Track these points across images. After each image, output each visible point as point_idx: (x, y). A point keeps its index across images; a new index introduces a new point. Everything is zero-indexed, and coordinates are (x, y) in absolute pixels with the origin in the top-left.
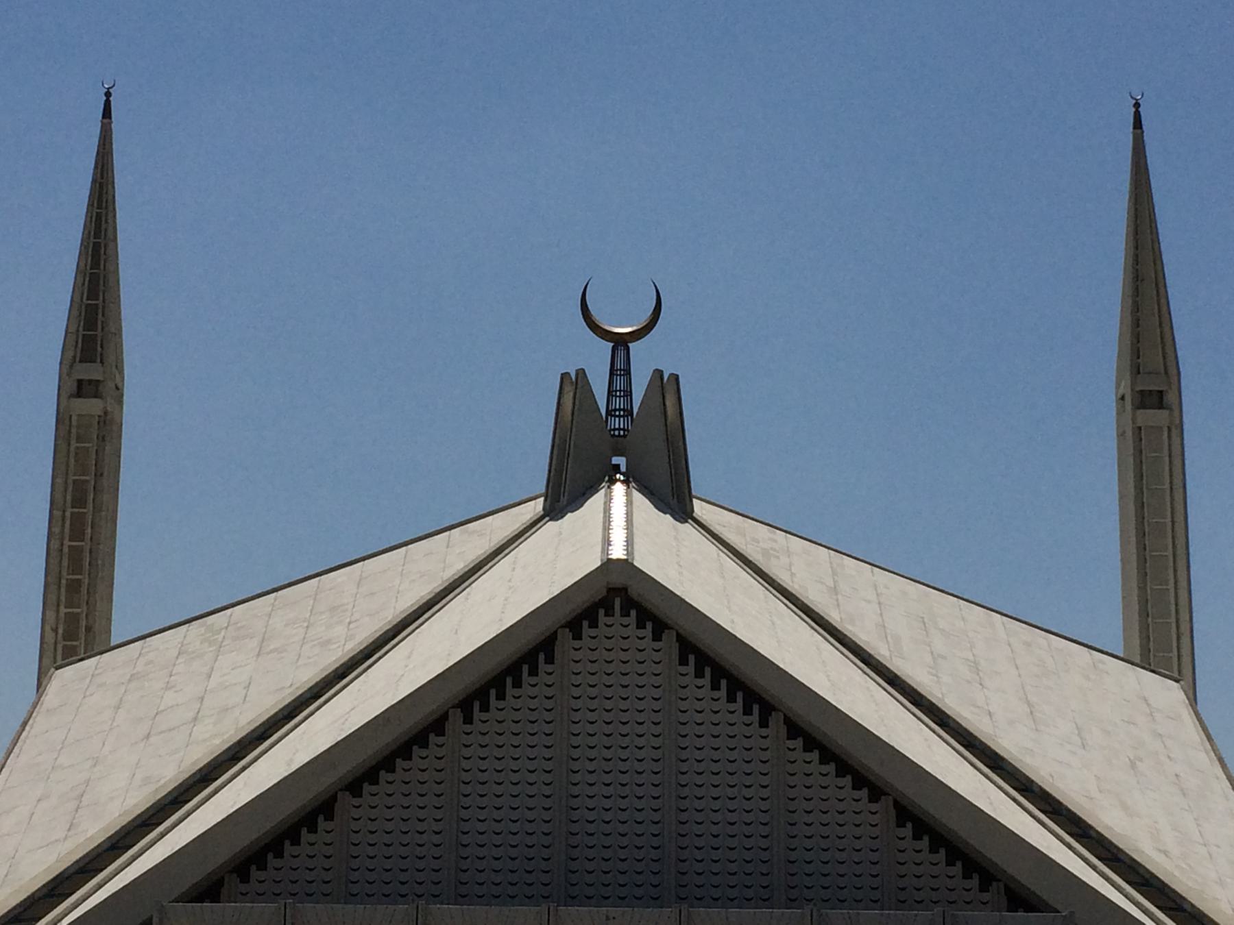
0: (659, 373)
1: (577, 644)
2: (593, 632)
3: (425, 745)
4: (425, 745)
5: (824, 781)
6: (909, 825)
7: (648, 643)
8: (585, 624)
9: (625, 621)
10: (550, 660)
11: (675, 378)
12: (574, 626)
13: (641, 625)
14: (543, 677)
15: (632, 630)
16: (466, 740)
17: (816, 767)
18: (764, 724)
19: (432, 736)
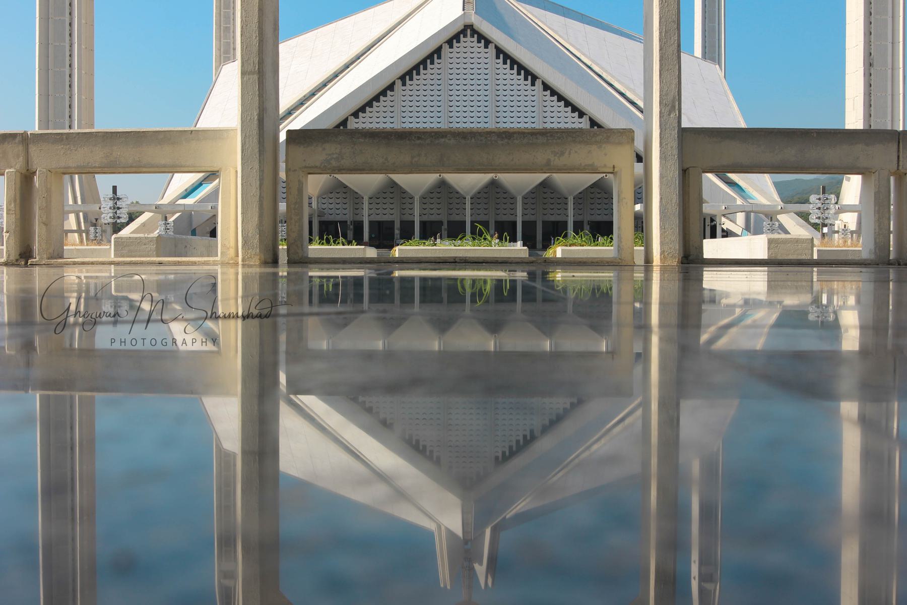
1: (451, 50)
2: (458, 45)
7: (482, 49)
8: (455, 41)
9: (472, 39)
10: (439, 57)
13: (479, 42)
14: (436, 65)
15: (475, 44)
16: (404, 93)
17: (556, 103)
18: (533, 84)
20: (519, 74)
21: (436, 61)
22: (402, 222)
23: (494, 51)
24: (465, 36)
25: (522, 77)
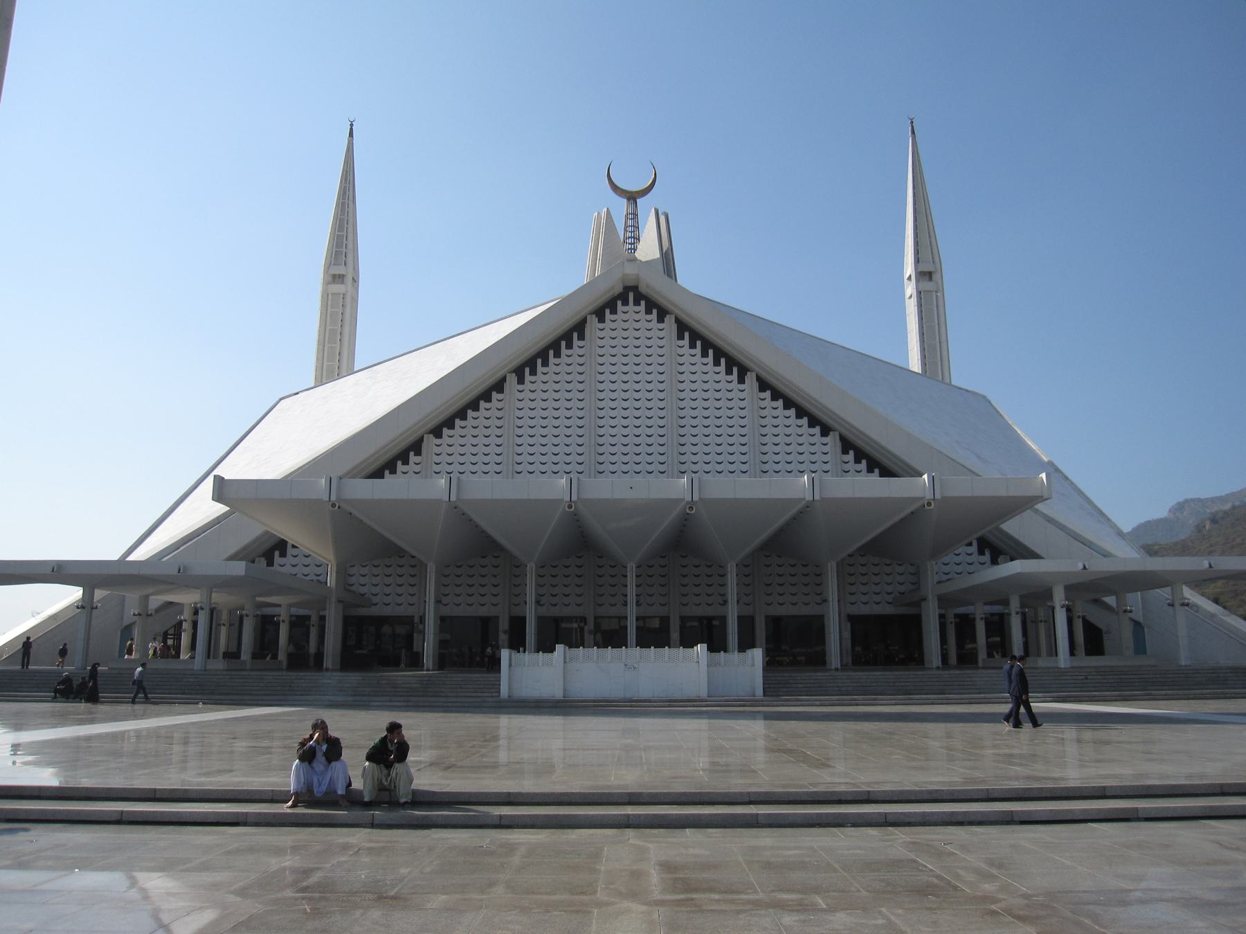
1: (601, 326)
2: (613, 317)
3: (489, 400)
6: (851, 452)
7: (654, 324)
8: (607, 311)
9: (637, 308)
10: (582, 337)
12: (600, 314)
13: (648, 312)
14: (576, 350)
15: (642, 315)
16: (520, 396)
17: (781, 411)
18: (741, 380)
19: (494, 394)
20: (717, 363)
21: (576, 342)
23: (675, 327)
24: (626, 303)
25: (722, 368)
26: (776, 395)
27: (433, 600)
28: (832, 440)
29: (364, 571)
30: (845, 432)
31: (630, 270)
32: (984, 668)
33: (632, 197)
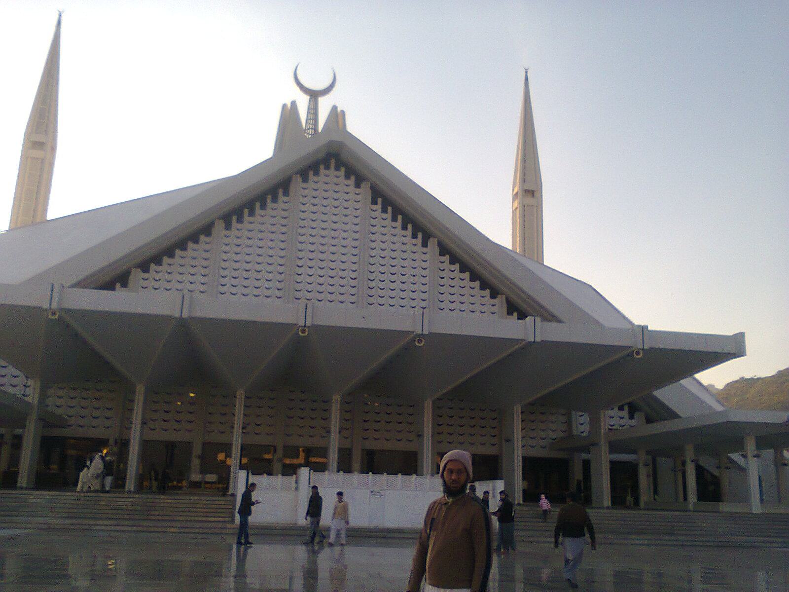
0: (335, 108)
1: (304, 185)
2: (316, 179)
3: (196, 241)
4: (196, 241)
5: (462, 283)
7: (352, 189)
8: (311, 173)
9: (337, 173)
10: (286, 193)
11: (343, 112)
12: (304, 174)
13: (347, 177)
14: (280, 205)
15: (341, 180)
17: (457, 274)
18: (425, 245)
21: (281, 198)
22: (205, 444)
23: (370, 193)
25: (409, 232)
26: (454, 260)
27: (139, 421)
28: (500, 301)
29: (61, 393)
30: (512, 296)
31: (336, 137)
32: (645, 509)
33: (314, 95)
